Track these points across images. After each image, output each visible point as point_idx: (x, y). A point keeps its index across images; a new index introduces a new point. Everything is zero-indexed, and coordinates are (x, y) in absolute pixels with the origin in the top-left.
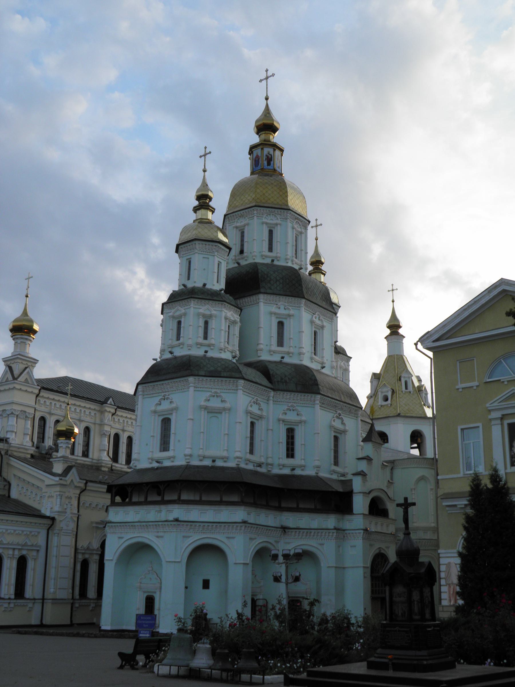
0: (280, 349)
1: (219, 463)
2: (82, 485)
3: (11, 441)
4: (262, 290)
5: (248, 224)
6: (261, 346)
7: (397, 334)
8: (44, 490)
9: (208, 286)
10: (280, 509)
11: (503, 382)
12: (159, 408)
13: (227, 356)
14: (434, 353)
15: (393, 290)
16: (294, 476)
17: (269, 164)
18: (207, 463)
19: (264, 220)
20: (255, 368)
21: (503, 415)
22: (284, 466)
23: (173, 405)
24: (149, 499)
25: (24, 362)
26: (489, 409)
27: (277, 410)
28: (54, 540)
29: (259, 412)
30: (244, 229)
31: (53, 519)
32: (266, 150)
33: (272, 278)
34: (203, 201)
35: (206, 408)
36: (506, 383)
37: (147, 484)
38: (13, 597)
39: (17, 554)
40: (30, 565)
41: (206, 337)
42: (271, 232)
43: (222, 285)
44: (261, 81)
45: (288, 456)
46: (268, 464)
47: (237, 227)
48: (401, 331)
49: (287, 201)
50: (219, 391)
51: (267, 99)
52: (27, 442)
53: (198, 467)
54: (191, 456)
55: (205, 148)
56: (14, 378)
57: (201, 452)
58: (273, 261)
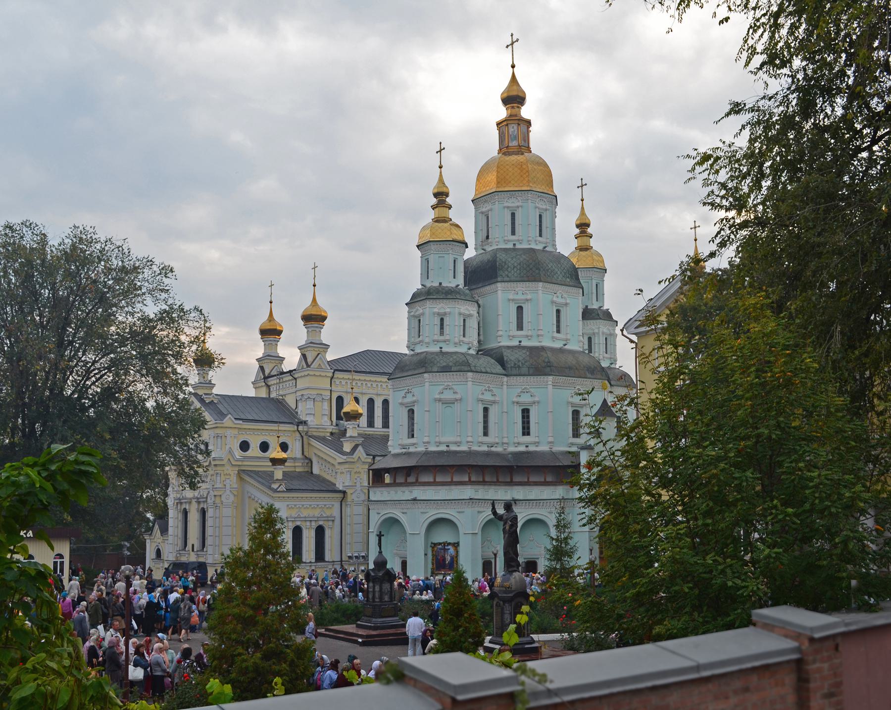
0: (520, 333)
1: (453, 448)
2: (370, 460)
3: (309, 423)
5: (491, 210)
6: (500, 333)
8: (337, 466)
9: (444, 285)
10: (511, 483)
12: (406, 400)
13: (463, 349)
16: (528, 453)
18: (443, 448)
19: (506, 204)
20: (491, 356)
22: (518, 444)
23: (414, 398)
24: (397, 481)
27: (509, 393)
28: (347, 511)
29: (492, 398)
31: (344, 492)
34: (441, 195)
35: (440, 400)
38: (314, 561)
39: (315, 525)
40: (327, 533)
41: (442, 333)
42: (513, 215)
43: (460, 281)
44: (507, 46)
45: (524, 434)
46: (503, 443)
47: (482, 213)
50: (450, 384)
51: (513, 66)
52: (325, 421)
53: (434, 452)
54: (428, 443)
56: (308, 366)
57: (437, 439)
58: (514, 245)
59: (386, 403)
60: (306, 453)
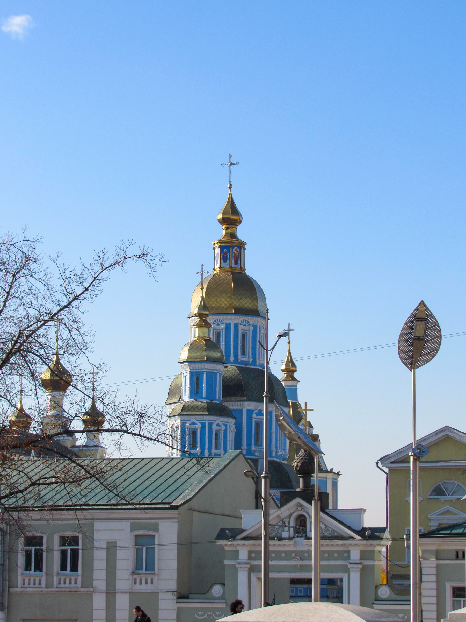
7: (293, 379)
11: (441, 500)
36: (443, 501)
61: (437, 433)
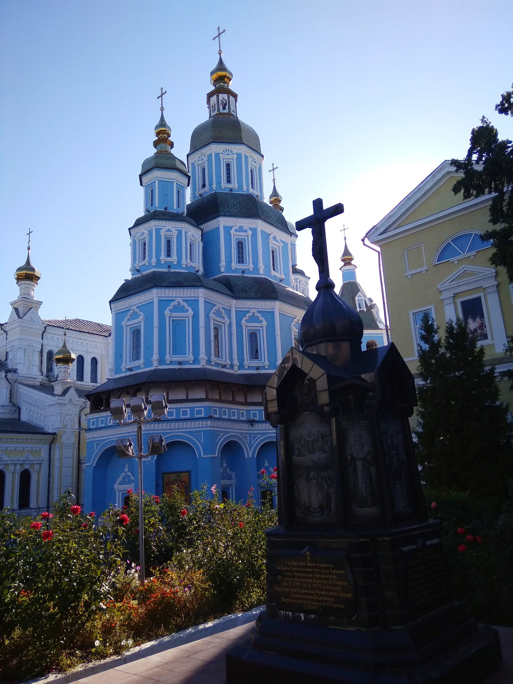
2: (81, 403)
4: (221, 213)
14: (380, 246)
15: (344, 230)
17: (224, 108)
21: (454, 294)
25: (28, 304)
26: (440, 290)
28: (56, 454)
30: (204, 166)
31: (54, 434)
32: (221, 96)
33: (230, 202)
34: (163, 137)
36: (456, 262)
37: (118, 389)
48: (353, 262)
49: (241, 137)
52: (35, 372)
55: (162, 89)
59: (94, 361)
60: (14, 401)
61: (433, 174)
